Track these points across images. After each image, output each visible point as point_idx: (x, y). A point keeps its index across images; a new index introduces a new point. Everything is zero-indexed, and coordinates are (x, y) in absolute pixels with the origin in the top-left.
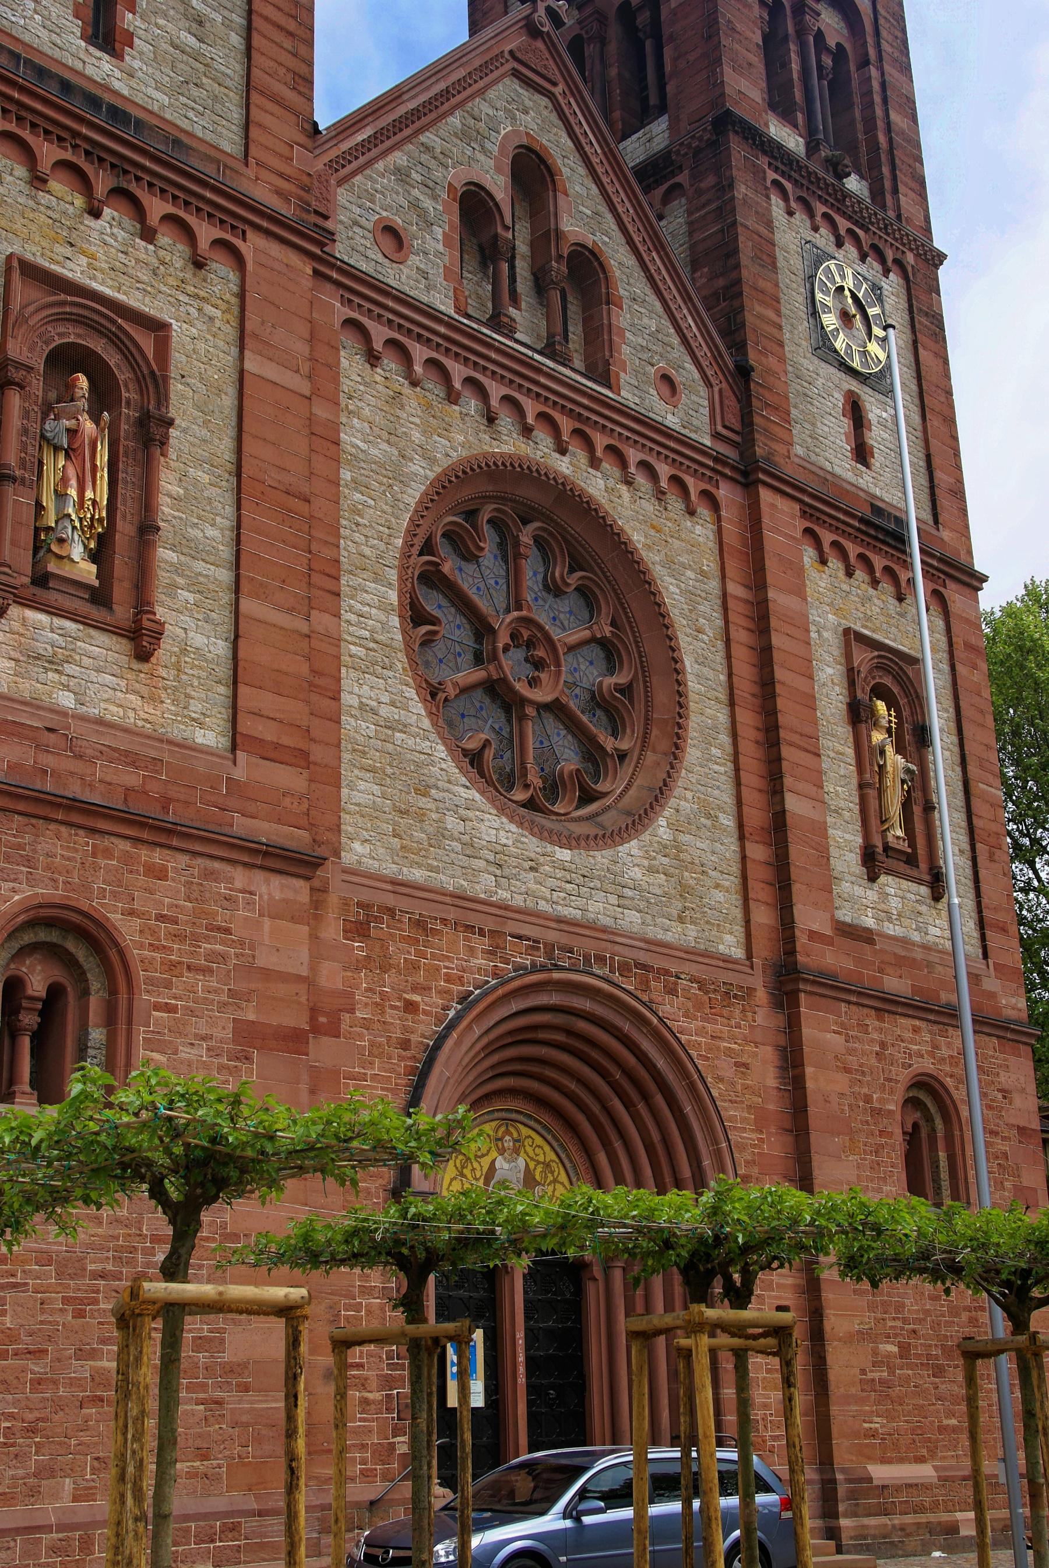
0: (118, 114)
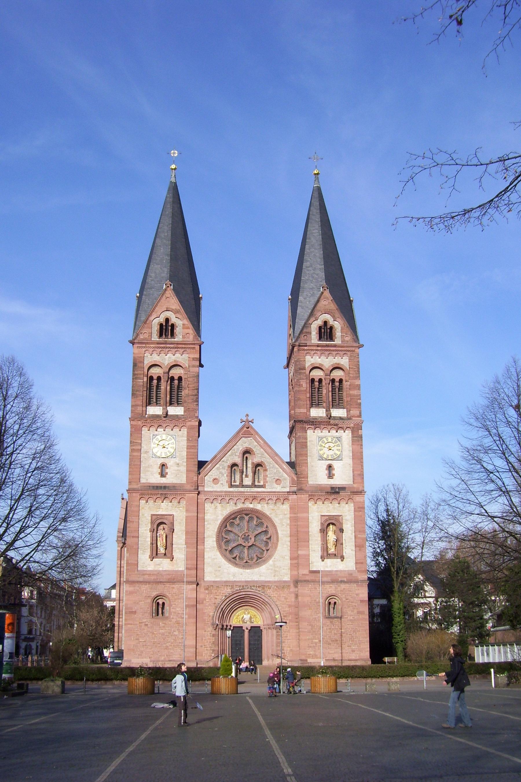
0: (165, 487)
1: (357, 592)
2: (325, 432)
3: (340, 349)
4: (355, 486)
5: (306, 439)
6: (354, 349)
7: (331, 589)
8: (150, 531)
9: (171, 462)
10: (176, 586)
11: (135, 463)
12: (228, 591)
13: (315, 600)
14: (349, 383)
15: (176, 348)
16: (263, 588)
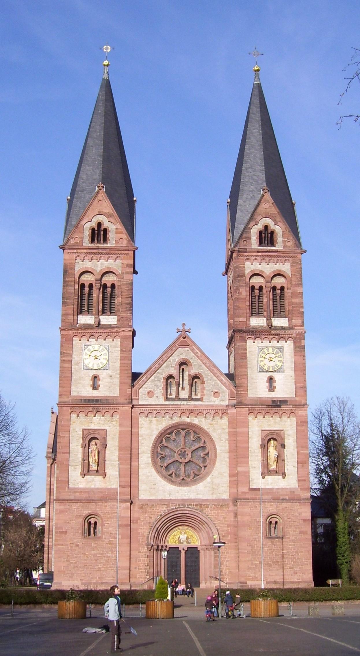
0: (97, 401)
1: (299, 511)
2: (266, 343)
3: (282, 255)
4: (297, 399)
5: (246, 349)
6: (296, 255)
7: (272, 508)
8: (82, 447)
9: (104, 374)
10: (109, 504)
11: (66, 375)
12: (164, 509)
13: (255, 520)
14: (290, 291)
15: (109, 254)
16: (201, 507)
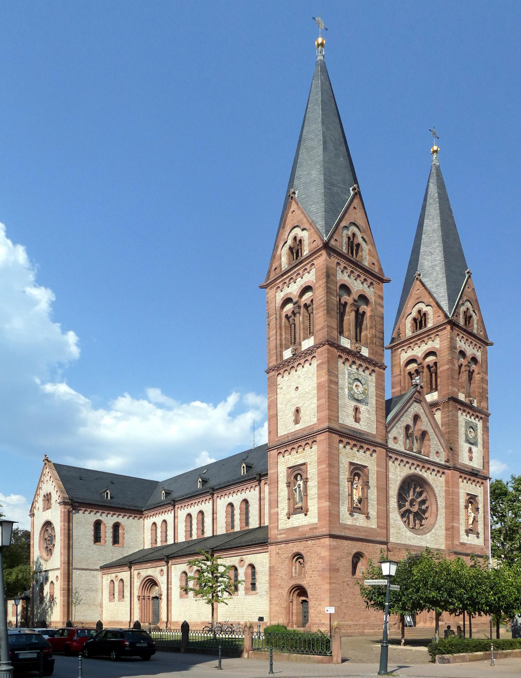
8: (348, 481)
